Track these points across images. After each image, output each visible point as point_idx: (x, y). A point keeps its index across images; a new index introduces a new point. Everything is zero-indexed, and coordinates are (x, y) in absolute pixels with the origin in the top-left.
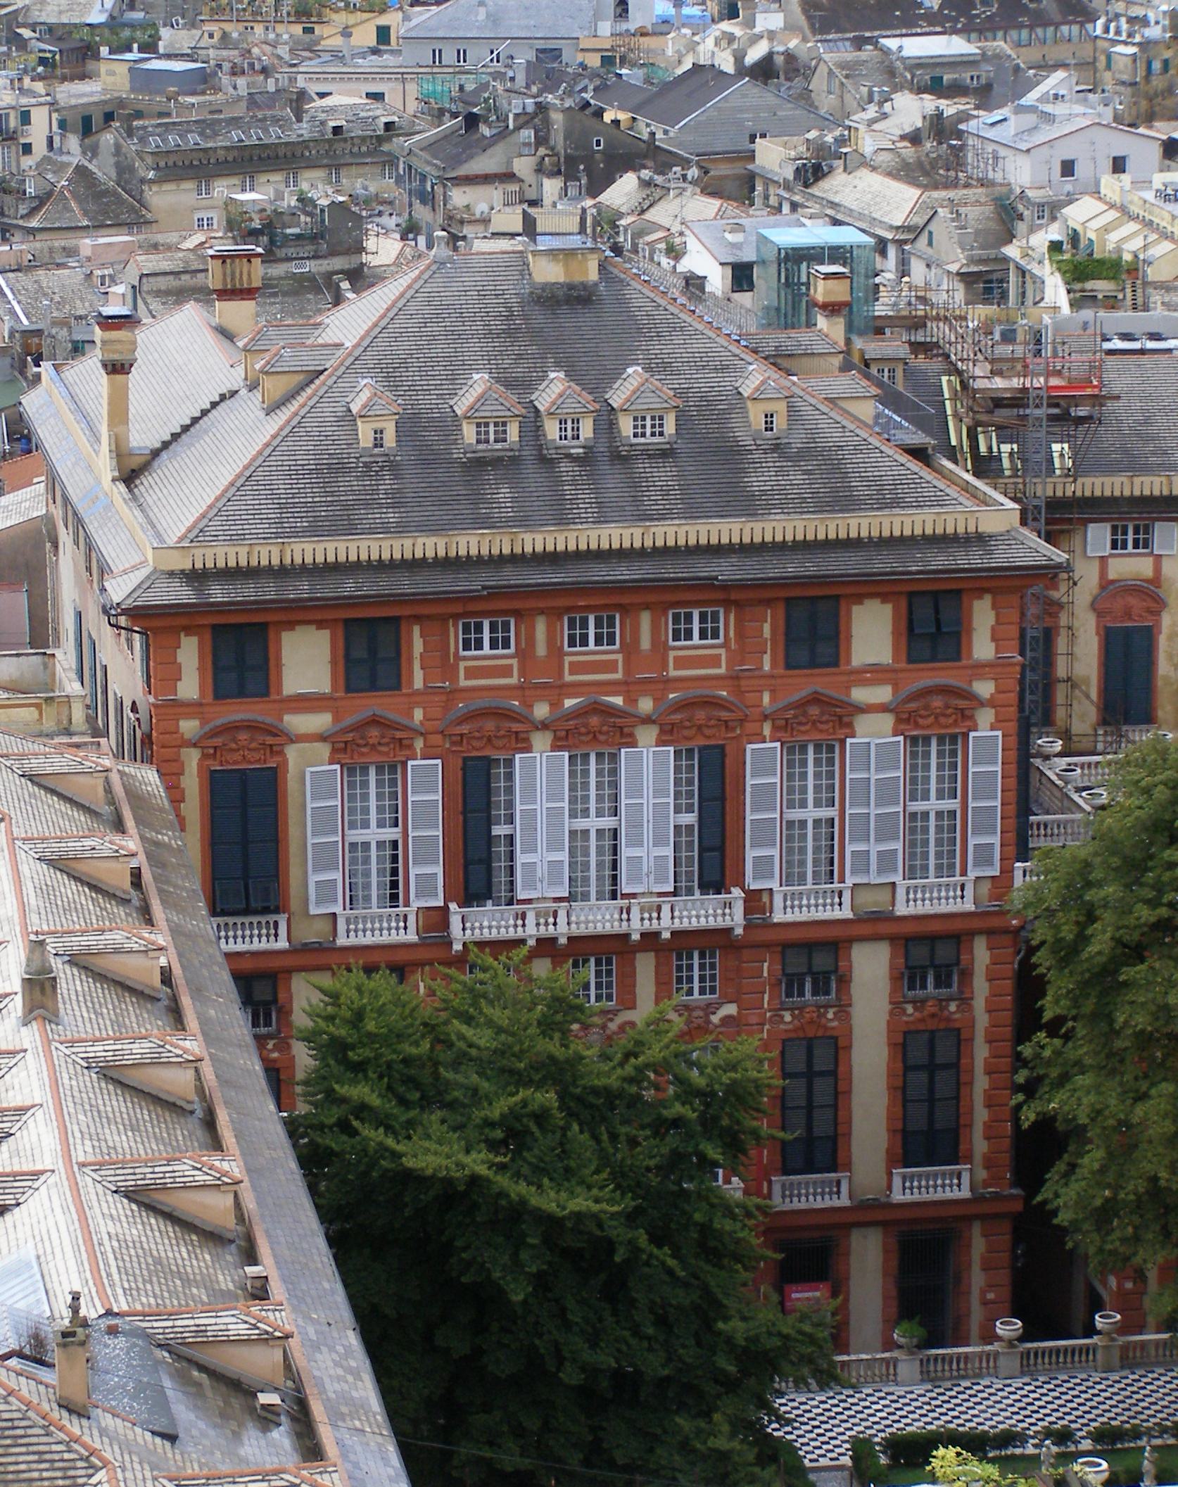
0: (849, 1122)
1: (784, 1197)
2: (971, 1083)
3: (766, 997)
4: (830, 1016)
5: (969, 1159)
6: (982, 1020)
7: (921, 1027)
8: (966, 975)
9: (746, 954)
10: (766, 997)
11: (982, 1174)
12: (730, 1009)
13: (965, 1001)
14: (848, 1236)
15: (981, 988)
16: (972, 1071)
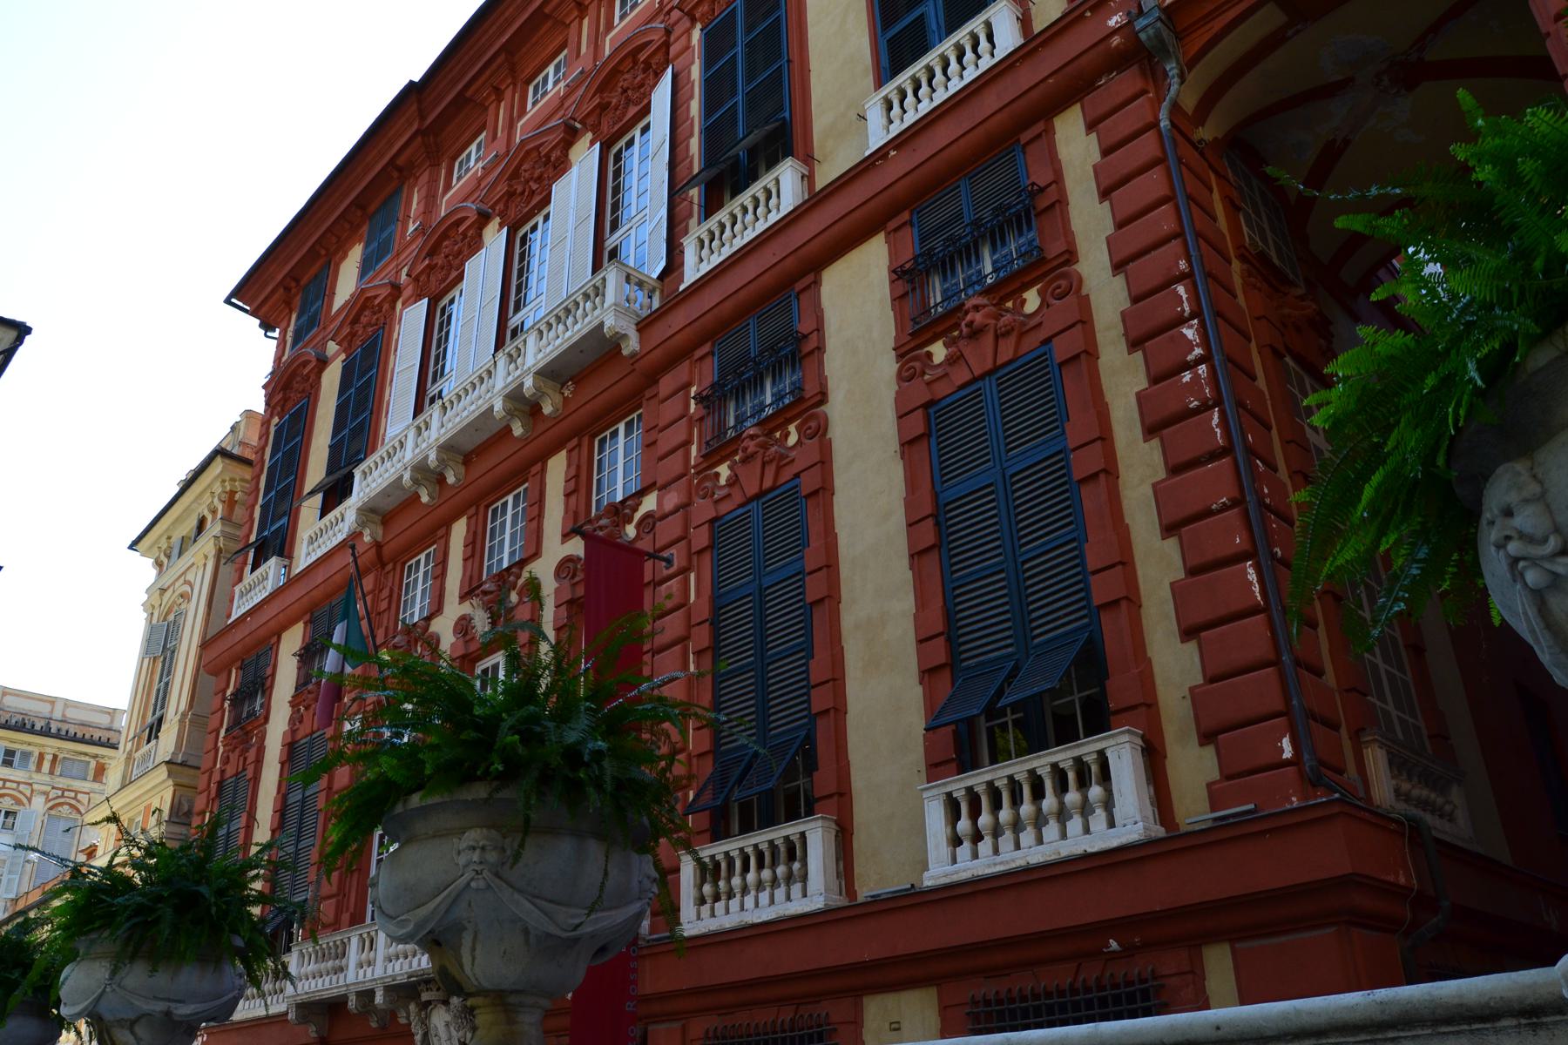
0: (837, 680)
1: (701, 901)
2: (1109, 471)
3: (694, 449)
4: (793, 439)
5: (1144, 714)
6: (1107, 295)
7: (961, 375)
8: (1039, 206)
9: (666, 384)
10: (694, 449)
11: (1194, 767)
12: (649, 503)
13: (1054, 268)
14: (857, 1022)
15: (1090, 221)
16: (1105, 437)
